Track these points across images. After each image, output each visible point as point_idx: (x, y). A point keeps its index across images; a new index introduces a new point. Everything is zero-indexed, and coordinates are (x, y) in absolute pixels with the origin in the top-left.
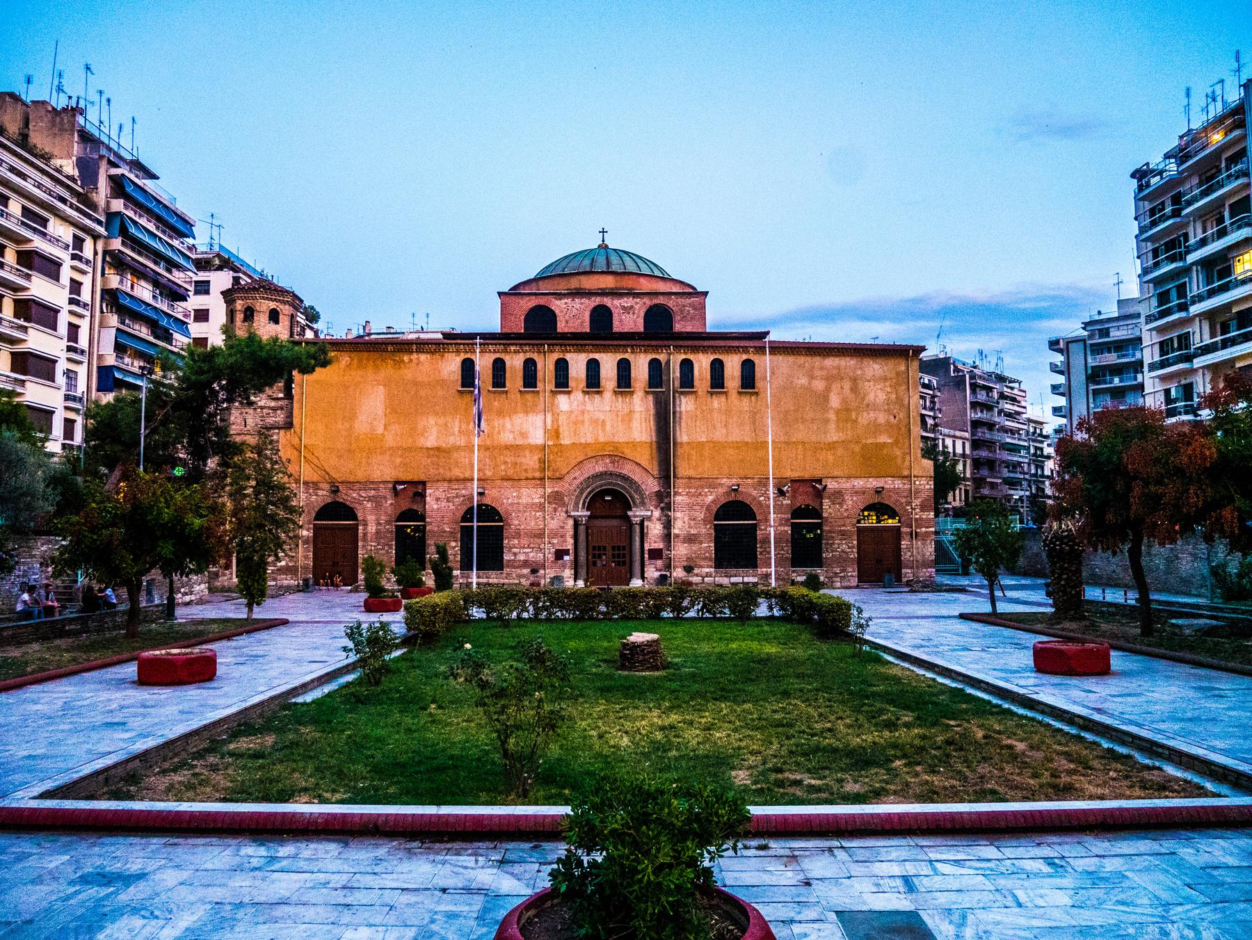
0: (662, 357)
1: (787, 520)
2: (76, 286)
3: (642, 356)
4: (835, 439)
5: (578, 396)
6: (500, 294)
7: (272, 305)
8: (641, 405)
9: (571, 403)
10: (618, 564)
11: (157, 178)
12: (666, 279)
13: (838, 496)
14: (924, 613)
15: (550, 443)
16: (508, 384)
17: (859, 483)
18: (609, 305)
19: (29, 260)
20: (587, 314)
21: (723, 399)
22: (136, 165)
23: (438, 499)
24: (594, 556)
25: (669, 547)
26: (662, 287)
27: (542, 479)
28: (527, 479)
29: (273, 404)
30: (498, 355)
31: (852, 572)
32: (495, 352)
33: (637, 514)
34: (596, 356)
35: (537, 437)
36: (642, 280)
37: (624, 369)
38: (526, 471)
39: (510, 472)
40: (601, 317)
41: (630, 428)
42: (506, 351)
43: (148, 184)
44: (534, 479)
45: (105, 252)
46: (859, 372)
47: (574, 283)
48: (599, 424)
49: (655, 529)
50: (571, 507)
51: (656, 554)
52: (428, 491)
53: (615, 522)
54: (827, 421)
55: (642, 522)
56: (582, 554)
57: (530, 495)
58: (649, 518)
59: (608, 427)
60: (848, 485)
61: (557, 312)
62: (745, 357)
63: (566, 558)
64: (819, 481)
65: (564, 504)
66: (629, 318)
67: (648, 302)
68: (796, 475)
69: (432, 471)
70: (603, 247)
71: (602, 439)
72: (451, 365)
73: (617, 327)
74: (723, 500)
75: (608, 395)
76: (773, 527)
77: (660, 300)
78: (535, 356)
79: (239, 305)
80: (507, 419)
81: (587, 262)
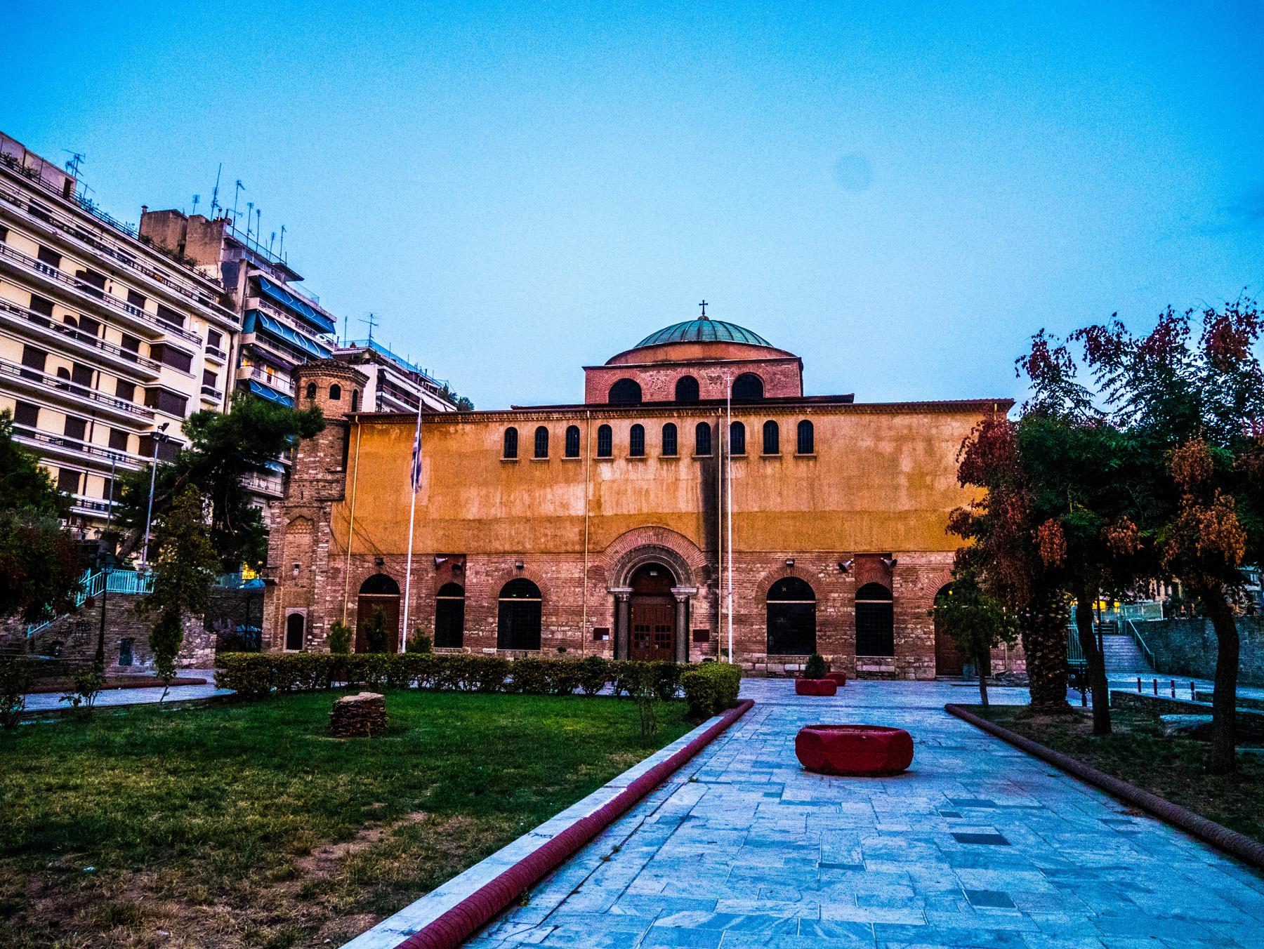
0: (710, 421)
1: (850, 600)
2: (210, 377)
3: (689, 420)
4: (906, 508)
5: (621, 463)
6: (585, 368)
7: (334, 381)
8: (687, 473)
9: (613, 472)
10: (662, 646)
11: (302, 279)
12: (770, 349)
13: (911, 573)
14: (926, 705)
15: (591, 514)
16: (550, 452)
17: (936, 558)
18: (695, 376)
19: (162, 353)
21: (777, 464)
22: (282, 269)
23: (477, 573)
24: (636, 636)
25: (715, 629)
26: (753, 355)
27: (582, 553)
28: (567, 552)
29: (329, 477)
30: (541, 424)
31: (930, 662)
32: (538, 420)
33: (681, 590)
34: (640, 421)
35: (578, 508)
36: (731, 349)
37: (670, 434)
38: (566, 544)
39: (551, 545)
40: (687, 389)
41: (675, 497)
42: (548, 419)
43: (291, 286)
44: (574, 552)
45: (242, 347)
46: (934, 431)
47: (661, 355)
48: (643, 493)
49: (701, 608)
50: (611, 583)
51: (701, 636)
52: (469, 565)
53: (659, 600)
54: (896, 488)
55: (687, 600)
56: (623, 634)
57: (571, 569)
58: (695, 596)
59: (652, 496)
60: (923, 561)
61: (642, 385)
62: (801, 418)
63: (606, 638)
64: (889, 556)
65: (605, 581)
66: (717, 384)
67: (737, 371)
68: (863, 548)
69: (474, 544)
70: (704, 318)
71: (645, 510)
72: (495, 436)
73: (703, 396)
74: (778, 577)
75: (652, 463)
76: (836, 606)
77: (750, 369)
78: (578, 423)
79: (304, 382)
80: (549, 490)
81: (678, 334)
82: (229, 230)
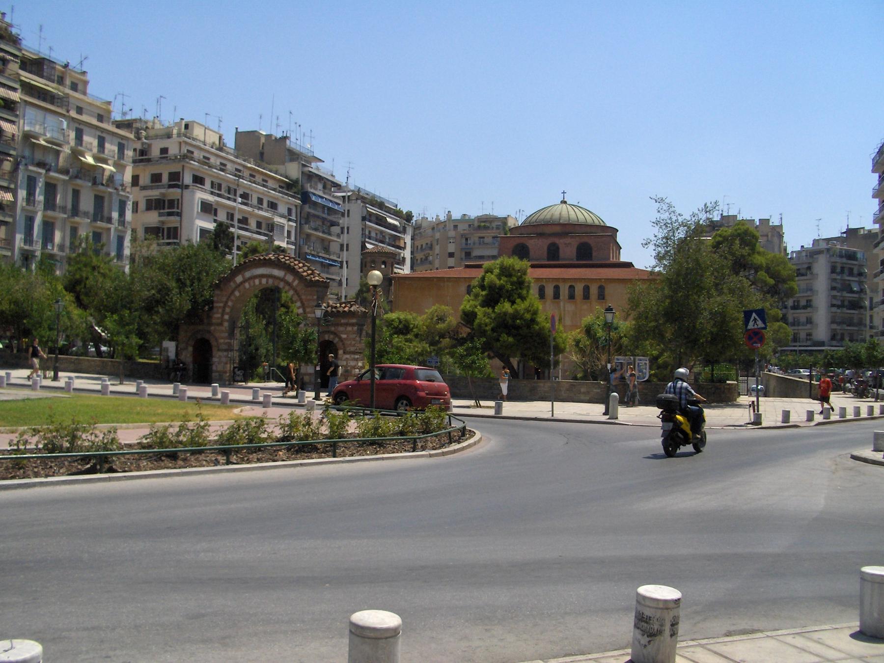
20: (546, 248)
47: (539, 230)
61: (530, 247)
62: (600, 284)
82: (288, 142)
